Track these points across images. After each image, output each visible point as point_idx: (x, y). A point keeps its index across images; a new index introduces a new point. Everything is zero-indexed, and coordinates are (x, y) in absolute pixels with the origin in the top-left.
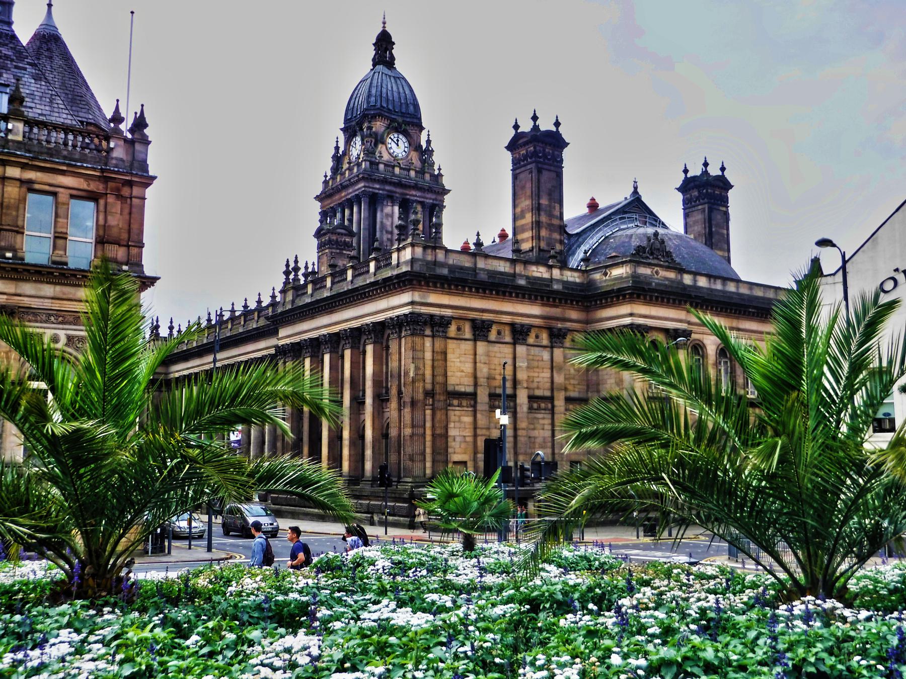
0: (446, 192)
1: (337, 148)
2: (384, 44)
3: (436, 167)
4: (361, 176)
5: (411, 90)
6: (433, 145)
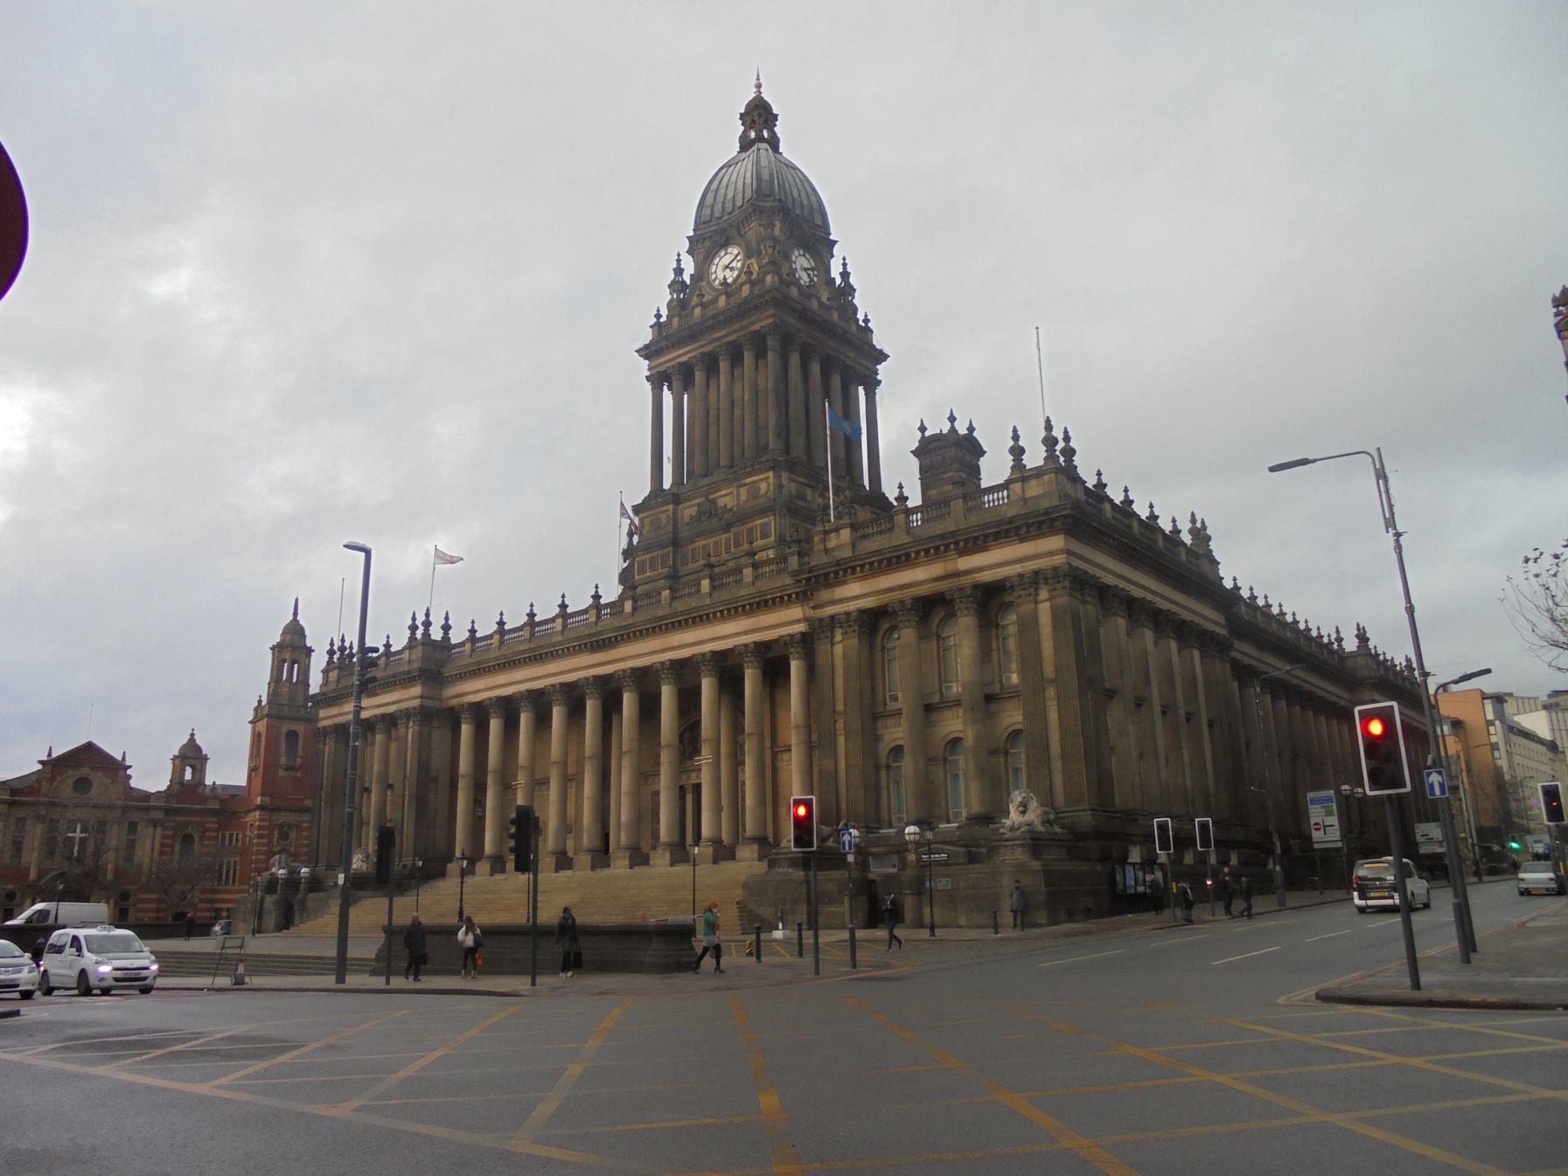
0: (882, 357)
1: (679, 271)
2: (759, 116)
3: (860, 316)
4: (768, 297)
5: (814, 190)
6: (852, 280)
